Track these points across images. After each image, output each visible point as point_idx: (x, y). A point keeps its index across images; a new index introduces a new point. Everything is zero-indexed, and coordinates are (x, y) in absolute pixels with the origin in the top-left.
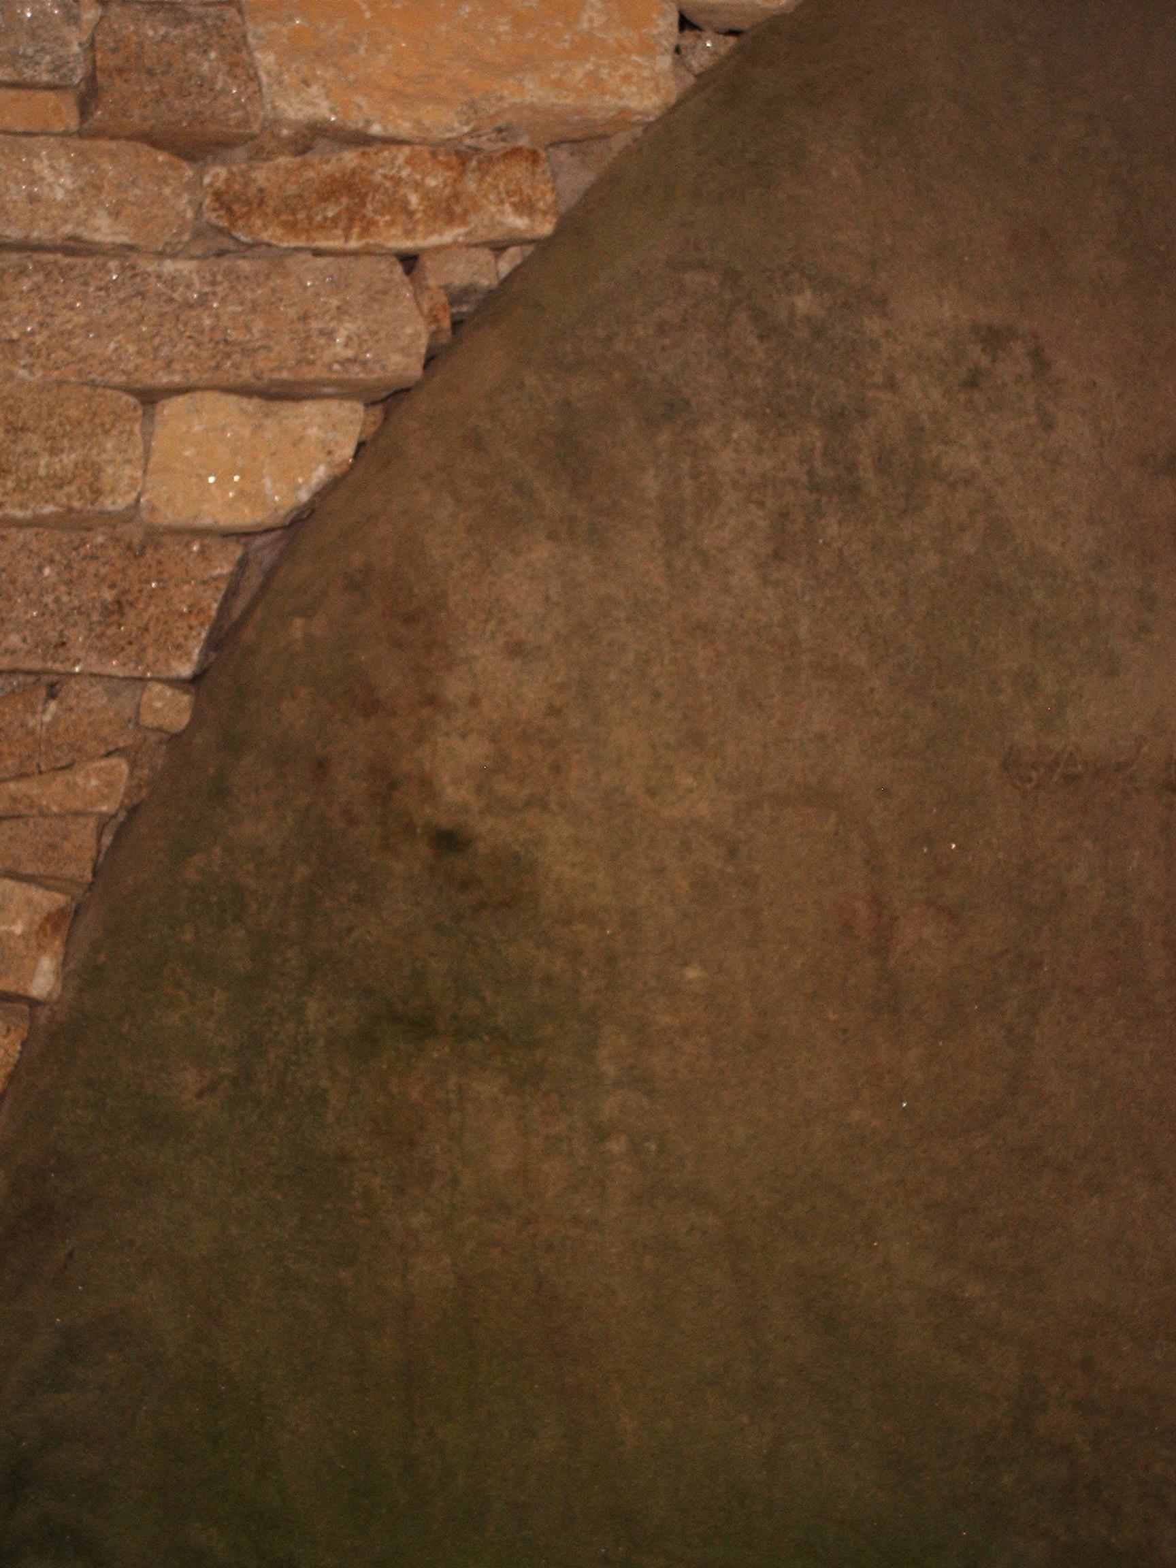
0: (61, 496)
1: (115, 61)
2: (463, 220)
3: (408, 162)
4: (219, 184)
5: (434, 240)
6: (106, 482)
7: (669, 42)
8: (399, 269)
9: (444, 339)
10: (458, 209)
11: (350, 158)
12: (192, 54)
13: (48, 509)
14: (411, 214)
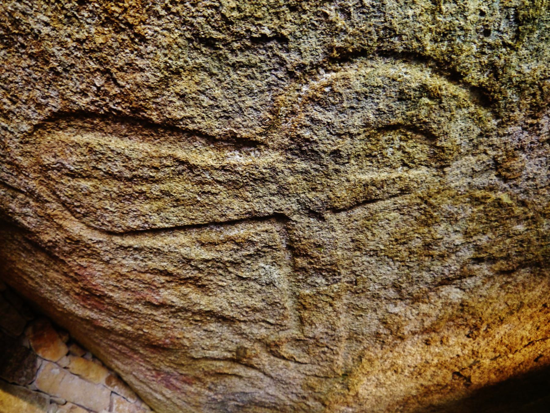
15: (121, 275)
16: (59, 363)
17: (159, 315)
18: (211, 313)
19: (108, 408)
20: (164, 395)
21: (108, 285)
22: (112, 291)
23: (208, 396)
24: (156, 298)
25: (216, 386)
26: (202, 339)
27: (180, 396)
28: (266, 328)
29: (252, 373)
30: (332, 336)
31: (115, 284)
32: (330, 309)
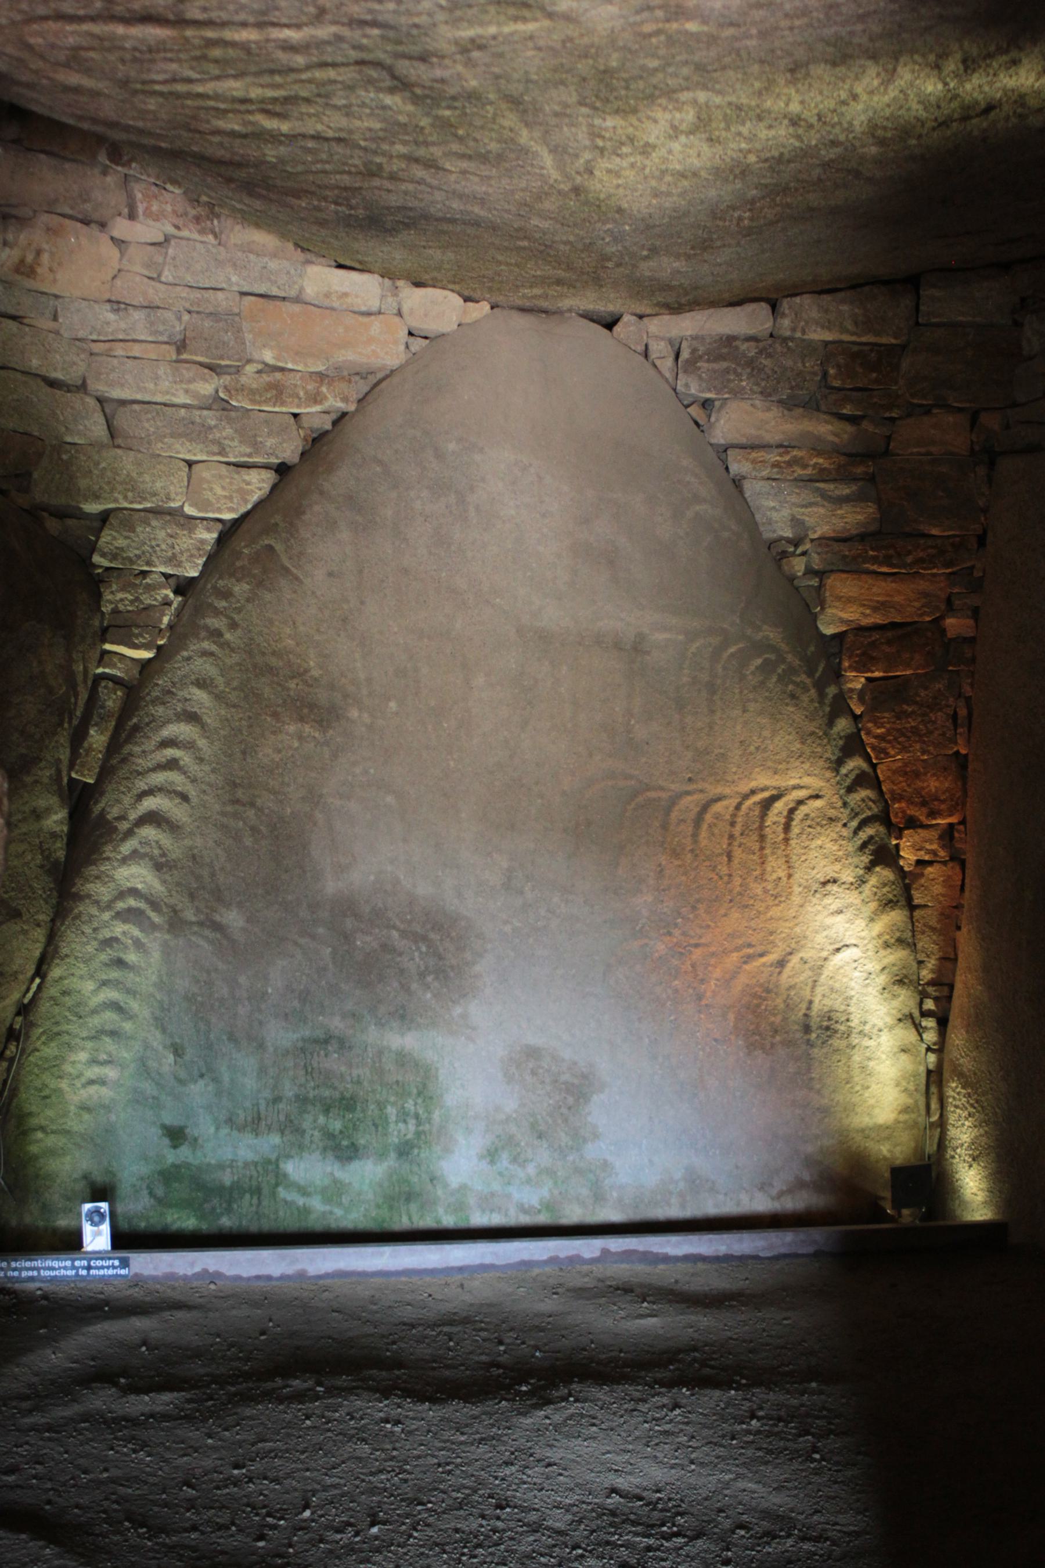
0: (154, 499)
2: (320, 403)
3: (301, 378)
4: (227, 383)
5: (308, 410)
6: (173, 496)
8: (292, 419)
9: (307, 448)
10: (319, 399)
11: (278, 375)
12: (222, 333)
13: (149, 505)
14: (300, 399)
19: (126, 211)
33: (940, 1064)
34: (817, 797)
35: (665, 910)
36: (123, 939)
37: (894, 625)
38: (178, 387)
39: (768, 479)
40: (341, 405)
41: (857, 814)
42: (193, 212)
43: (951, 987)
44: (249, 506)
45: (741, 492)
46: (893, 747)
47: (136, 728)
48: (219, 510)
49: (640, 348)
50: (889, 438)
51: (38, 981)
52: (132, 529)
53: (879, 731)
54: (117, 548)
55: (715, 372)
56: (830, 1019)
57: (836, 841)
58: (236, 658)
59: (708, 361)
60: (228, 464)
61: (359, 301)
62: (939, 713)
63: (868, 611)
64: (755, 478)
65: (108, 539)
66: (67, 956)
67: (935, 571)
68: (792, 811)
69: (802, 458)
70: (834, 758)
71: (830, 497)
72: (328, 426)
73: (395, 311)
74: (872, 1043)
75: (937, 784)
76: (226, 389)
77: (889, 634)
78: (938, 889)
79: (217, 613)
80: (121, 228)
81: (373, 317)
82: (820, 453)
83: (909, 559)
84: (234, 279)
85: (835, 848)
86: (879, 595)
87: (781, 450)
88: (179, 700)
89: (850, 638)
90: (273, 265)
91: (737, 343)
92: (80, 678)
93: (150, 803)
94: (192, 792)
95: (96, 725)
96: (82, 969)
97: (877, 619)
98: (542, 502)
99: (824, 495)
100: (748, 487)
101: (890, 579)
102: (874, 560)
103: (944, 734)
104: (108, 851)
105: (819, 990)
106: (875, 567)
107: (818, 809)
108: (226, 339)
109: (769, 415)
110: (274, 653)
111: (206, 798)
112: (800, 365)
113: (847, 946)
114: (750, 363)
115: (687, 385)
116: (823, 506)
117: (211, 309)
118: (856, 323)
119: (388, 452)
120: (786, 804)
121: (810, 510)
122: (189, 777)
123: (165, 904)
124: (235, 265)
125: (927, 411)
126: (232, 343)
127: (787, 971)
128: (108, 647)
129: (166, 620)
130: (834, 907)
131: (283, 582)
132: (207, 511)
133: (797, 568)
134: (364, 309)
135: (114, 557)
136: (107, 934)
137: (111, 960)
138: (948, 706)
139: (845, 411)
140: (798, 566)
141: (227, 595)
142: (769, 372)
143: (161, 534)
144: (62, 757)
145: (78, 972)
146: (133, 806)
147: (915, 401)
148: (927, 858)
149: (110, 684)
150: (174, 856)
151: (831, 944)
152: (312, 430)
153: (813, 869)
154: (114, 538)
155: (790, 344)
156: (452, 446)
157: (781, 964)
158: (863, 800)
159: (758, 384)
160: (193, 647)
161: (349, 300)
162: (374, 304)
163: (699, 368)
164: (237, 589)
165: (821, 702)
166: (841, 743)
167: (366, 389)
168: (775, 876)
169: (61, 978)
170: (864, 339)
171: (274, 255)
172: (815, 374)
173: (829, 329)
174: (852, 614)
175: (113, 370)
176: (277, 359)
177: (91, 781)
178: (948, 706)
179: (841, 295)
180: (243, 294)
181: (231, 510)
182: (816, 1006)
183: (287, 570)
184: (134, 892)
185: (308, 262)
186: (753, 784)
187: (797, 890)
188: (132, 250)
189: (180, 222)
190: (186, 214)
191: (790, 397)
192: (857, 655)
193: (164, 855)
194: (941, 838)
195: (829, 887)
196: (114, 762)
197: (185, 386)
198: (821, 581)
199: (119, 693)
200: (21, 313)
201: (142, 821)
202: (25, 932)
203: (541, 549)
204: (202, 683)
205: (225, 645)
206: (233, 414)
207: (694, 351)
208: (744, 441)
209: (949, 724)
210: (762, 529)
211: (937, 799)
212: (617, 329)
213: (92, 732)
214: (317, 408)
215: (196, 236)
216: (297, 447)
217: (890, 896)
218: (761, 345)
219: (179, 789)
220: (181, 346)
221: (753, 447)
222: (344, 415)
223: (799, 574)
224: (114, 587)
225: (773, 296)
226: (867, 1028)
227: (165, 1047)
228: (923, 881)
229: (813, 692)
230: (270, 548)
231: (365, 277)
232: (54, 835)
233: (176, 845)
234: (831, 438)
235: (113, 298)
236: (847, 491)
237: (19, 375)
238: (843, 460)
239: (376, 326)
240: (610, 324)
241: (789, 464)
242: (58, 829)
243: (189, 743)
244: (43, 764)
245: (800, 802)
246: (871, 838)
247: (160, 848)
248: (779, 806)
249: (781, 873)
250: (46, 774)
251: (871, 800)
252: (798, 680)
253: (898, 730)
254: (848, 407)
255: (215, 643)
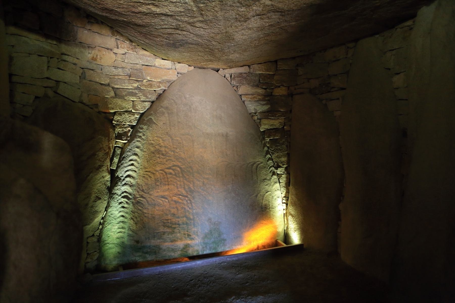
1: (132, 74)
4: (140, 84)
7: (176, 75)
8: (154, 91)
9: (157, 97)
11: (151, 82)
12: (138, 73)
15: (120, 4)
16: (86, 27)
17: (139, 15)
18: (162, 14)
19: (116, 47)
20: (144, 42)
21: (114, 7)
22: (116, 8)
23: (166, 42)
24: (136, 10)
25: (169, 38)
26: (159, 22)
27: (153, 42)
28: (187, 17)
29: (185, 33)
30: (217, 19)
31: (118, 6)
32: (213, 11)
33: (287, 213)
34: (262, 163)
35: (234, 188)
36: (124, 202)
37: (274, 129)
38: (129, 85)
39: (250, 101)
40: (164, 88)
41: (269, 166)
42: (131, 47)
43: (288, 198)
44: (146, 110)
45: (244, 104)
46: (275, 152)
47: (124, 157)
48: (140, 111)
49: (224, 76)
50: (272, 92)
51: (106, 212)
52: (121, 115)
53: (272, 149)
54: (118, 119)
55: (239, 80)
56: (266, 206)
57: (265, 171)
58: (145, 142)
59: (237, 78)
60: (141, 101)
61: (167, 66)
62: (284, 145)
63: (269, 126)
64: (247, 101)
65: (116, 118)
66: (112, 206)
67: (282, 118)
68: (257, 166)
69: (256, 97)
70: (264, 155)
71: (261, 104)
72: (162, 93)
73: (175, 69)
74: (274, 210)
75: (284, 159)
76: (140, 85)
77: (274, 130)
78: (285, 179)
79: (140, 132)
80: (116, 50)
81: (170, 70)
82: (259, 96)
83: (277, 116)
84: (141, 62)
85: (266, 173)
86: (272, 123)
87: (252, 95)
88: (133, 151)
89: (266, 131)
90: (149, 59)
91: (243, 74)
92: (111, 147)
93: (128, 173)
94: (136, 170)
95: (115, 157)
96: (115, 209)
97: (271, 127)
98: (206, 107)
99: (260, 104)
100: (246, 102)
101: (273, 120)
102: (270, 116)
103: (285, 149)
104: (119, 183)
105: (264, 200)
106: (270, 118)
107: (262, 165)
108: (139, 74)
109: (250, 88)
110: (153, 140)
111: (140, 171)
112: (255, 78)
113: (268, 191)
114: (245, 78)
115: (233, 83)
116: (260, 106)
117: (136, 68)
118: (265, 70)
119: (175, 98)
120: (256, 165)
121: (257, 107)
122: (136, 167)
123: (132, 194)
124: (141, 59)
125: (279, 87)
126: (141, 75)
127: (258, 197)
128: (117, 140)
129: (129, 134)
130: (266, 184)
131: (154, 125)
132: (137, 111)
133: (256, 118)
134: (168, 68)
135: (117, 121)
136: (120, 201)
137: (121, 207)
138: (286, 144)
139: (263, 87)
140: (256, 118)
141: (142, 129)
142: (249, 80)
143: (127, 116)
144: (108, 164)
145: (114, 210)
146: (124, 174)
147: (277, 85)
148: (282, 173)
149: (118, 148)
150: (134, 184)
151: (266, 191)
152: (159, 94)
153: (262, 177)
154: (117, 118)
155: (253, 74)
156: (188, 96)
157: (257, 196)
158: (270, 163)
159: (247, 82)
160: (136, 140)
161: (165, 66)
162: (170, 67)
163: (235, 79)
164: (144, 127)
165: (262, 144)
166: (265, 152)
167: (169, 85)
168: (255, 179)
169: (111, 211)
170: (267, 73)
171: (149, 57)
172: (258, 80)
173: (260, 71)
174: (267, 127)
175: (115, 81)
176: (151, 78)
177: (115, 169)
178: (286, 144)
179: (262, 64)
180: (143, 65)
181: (142, 111)
182: (263, 203)
183: (155, 123)
184: (125, 192)
185: (156, 58)
186: (250, 161)
187: (259, 181)
188: (118, 55)
189: (128, 49)
190: (129, 48)
191: (253, 85)
192: (268, 135)
193: (132, 184)
194: (285, 169)
195: (265, 180)
196: (120, 165)
197: (131, 85)
198: (260, 120)
199: (120, 150)
200: (94, 69)
201: (126, 177)
202: (102, 202)
203: (206, 116)
204: (138, 147)
205: (143, 139)
206: (142, 90)
207: (234, 76)
208: (245, 94)
209: (286, 147)
210: (249, 111)
211: (284, 162)
212: (219, 72)
213: (115, 159)
214: (160, 89)
215: (132, 52)
216: (155, 97)
217: (276, 181)
218: (247, 74)
219: (134, 170)
220: (130, 76)
221: (246, 95)
222: (165, 90)
223: (256, 119)
224: (118, 128)
225: (249, 65)
226: (273, 207)
227: (134, 224)
228: (282, 178)
229: (260, 143)
230: (151, 118)
231: (168, 61)
232: (107, 181)
233: (134, 181)
234: (261, 93)
235: (114, 66)
236: (265, 103)
237: (94, 83)
238: (263, 97)
239: (171, 72)
240: (217, 71)
241: (253, 98)
242: (108, 180)
243: (135, 160)
244: (104, 167)
245: (259, 164)
246: (272, 170)
247: (131, 182)
248: (255, 165)
249: (256, 178)
250: (105, 168)
251: (271, 163)
252: (257, 140)
253: (276, 149)
254: (264, 86)
255: (140, 139)
